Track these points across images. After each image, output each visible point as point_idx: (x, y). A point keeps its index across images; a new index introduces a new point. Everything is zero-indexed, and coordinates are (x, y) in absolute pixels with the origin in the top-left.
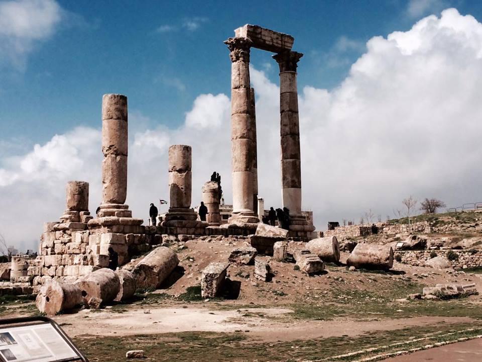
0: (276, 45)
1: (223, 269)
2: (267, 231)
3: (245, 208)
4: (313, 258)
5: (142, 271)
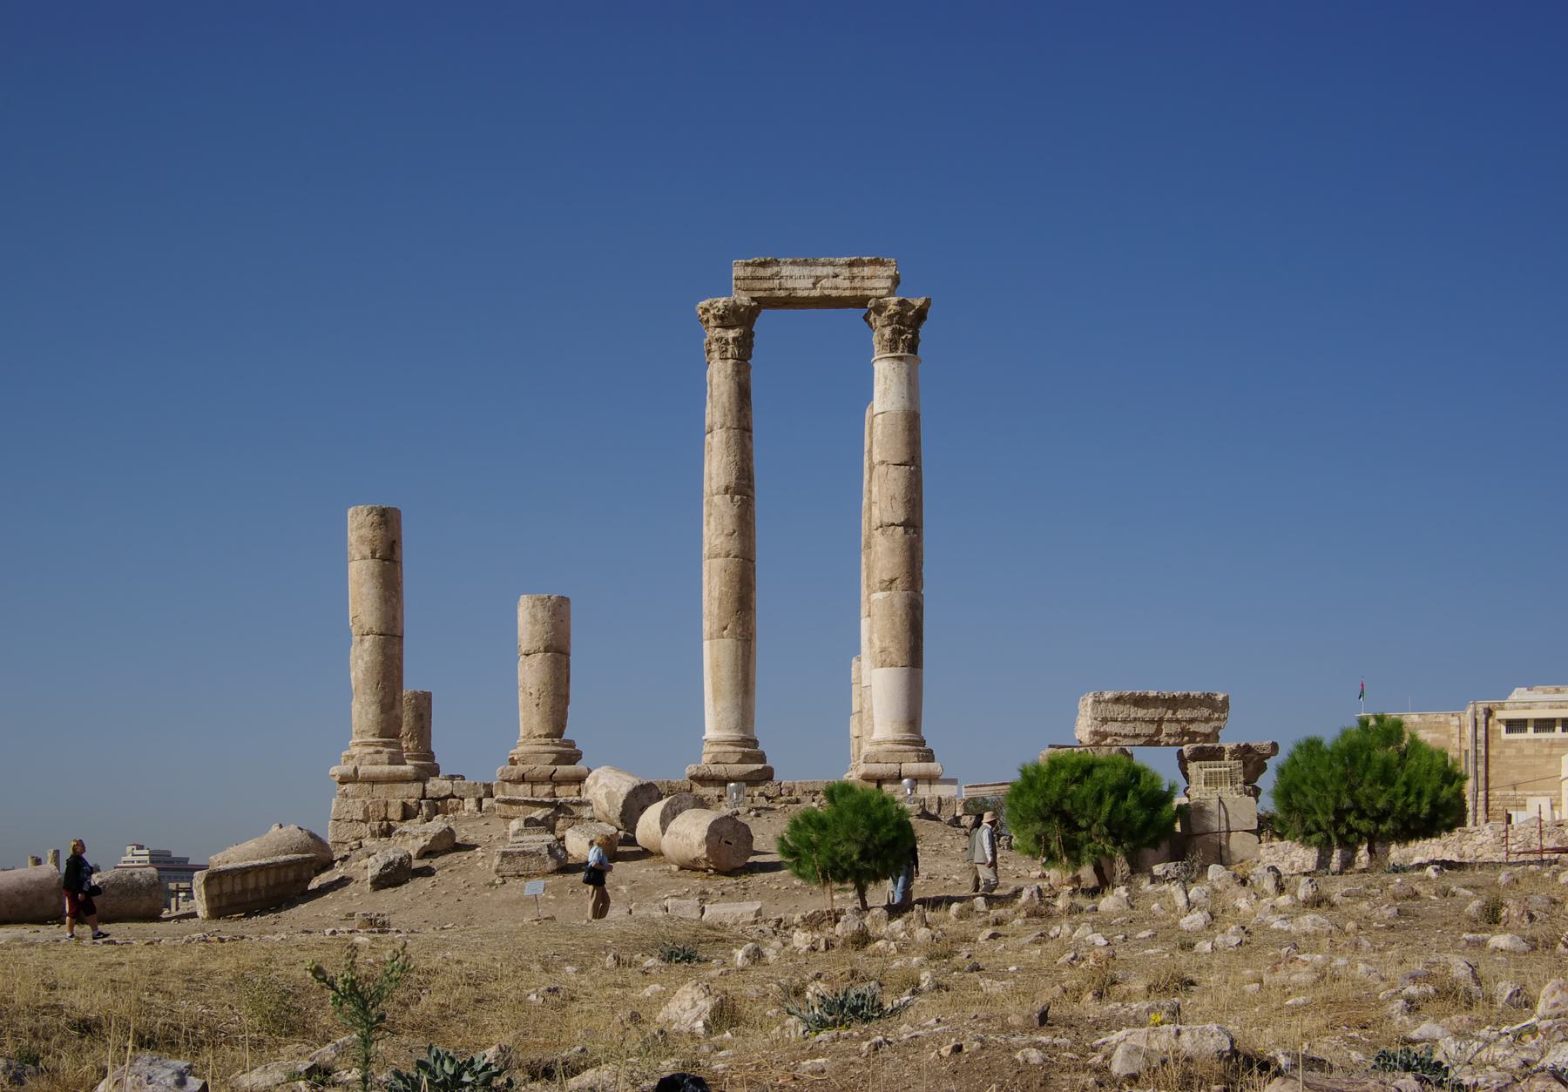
0: (834, 293)
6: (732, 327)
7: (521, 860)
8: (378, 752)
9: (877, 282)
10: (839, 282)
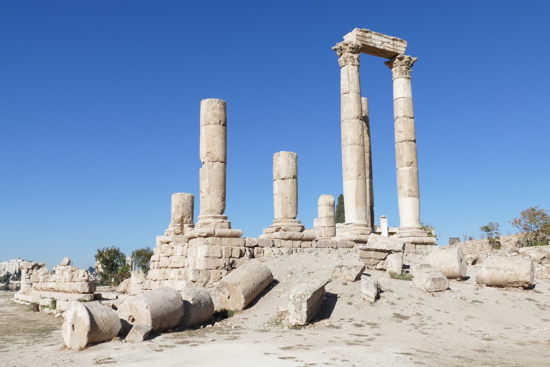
0: (388, 49)
1: (321, 286)
2: (379, 243)
3: (358, 219)
4: (435, 273)
5: (225, 289)
6: (355, 53)
7: (438, 282)
8: (223, 222)
9: (401, 47)
10: (389, 45)
